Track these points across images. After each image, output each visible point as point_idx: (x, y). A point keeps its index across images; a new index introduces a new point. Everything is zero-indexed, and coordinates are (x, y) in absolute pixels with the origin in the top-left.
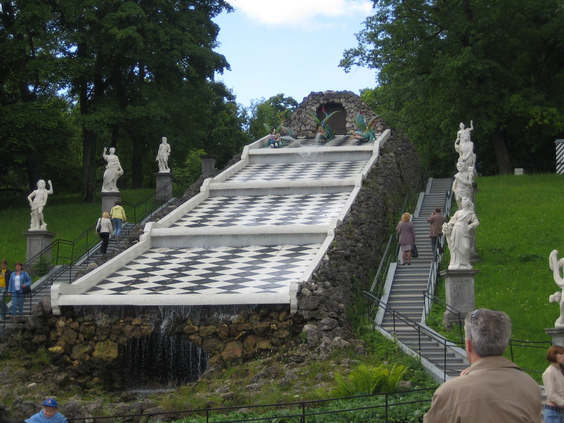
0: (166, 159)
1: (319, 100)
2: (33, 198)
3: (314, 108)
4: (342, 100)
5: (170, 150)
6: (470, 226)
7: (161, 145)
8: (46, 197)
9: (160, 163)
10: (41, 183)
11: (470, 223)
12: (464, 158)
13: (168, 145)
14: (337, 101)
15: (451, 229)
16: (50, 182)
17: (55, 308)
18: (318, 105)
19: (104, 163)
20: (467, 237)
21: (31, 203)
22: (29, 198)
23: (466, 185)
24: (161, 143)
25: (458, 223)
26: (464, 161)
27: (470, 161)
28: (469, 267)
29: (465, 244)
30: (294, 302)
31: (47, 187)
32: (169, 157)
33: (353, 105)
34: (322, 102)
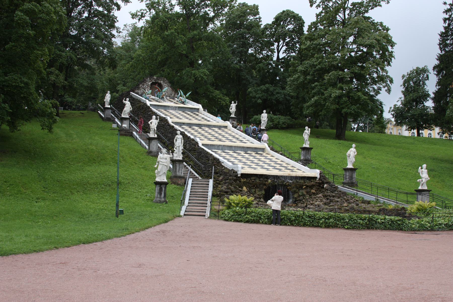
1: (152, 81)
2: (151, 123)
3: (150, 83)
4: (162, 82)
7: (107, 94)
8: (157, 123)
9: (106, 103)
11: (355, 153)
13: (110, 95)
14: (159, 82)
17: (239, 174)
18: (151, 82)
19: (124, 105)
21: (151, 125)
22: (149, 123)
23: (308, 135)
24: (107, 93)
26: (264, 121)
28: (353, 167)
30: (318, 177)
33: (166, 85)
34: (153, 81)
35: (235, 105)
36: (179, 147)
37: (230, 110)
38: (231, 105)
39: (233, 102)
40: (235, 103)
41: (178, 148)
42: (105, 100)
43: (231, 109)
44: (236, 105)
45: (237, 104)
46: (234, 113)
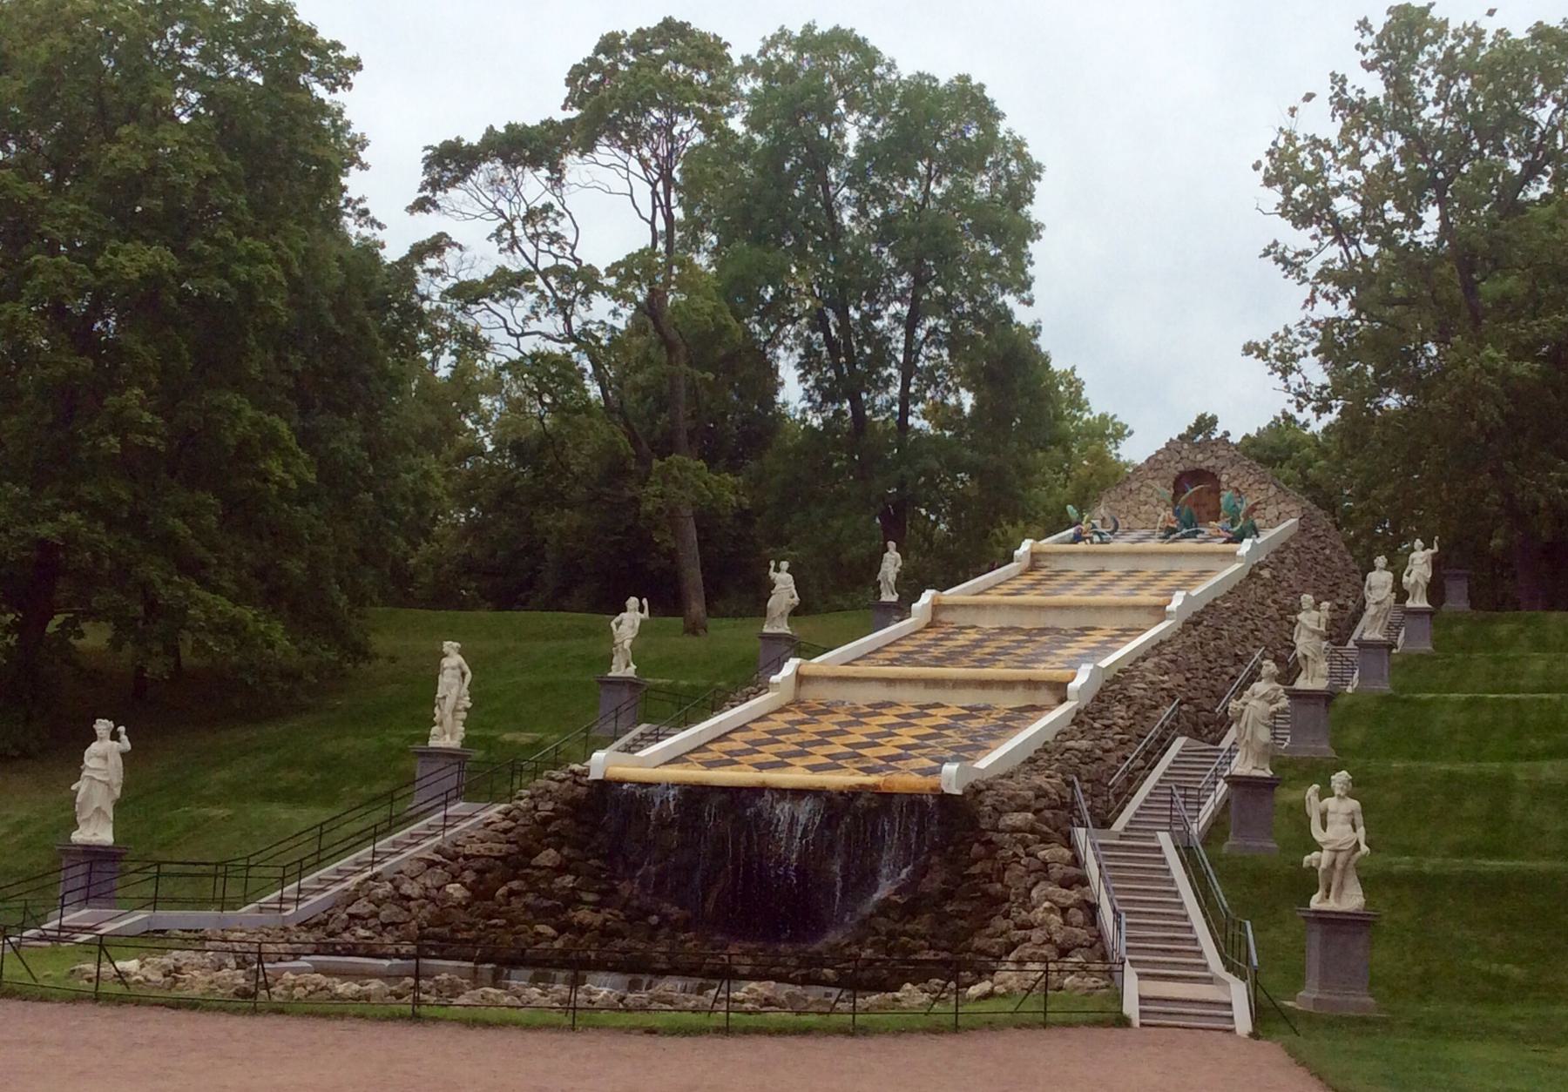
0: (892, 577)
5: (900, 564)
6: (1273, 708)
7: (886, 555)
9: (882, 585)
10: (633, 602)
12: (1379, 599)
13: (898, 555)
15: (1242, 711)
16: (645, 601)
20: (1265, 725)
24: (887, 551)
25: (1253, 703)
27: (1386, 605)
29: (1264, 735)
31: (641, 610)
32: (898, 575)
35: (1429, 551)
36: (444, 698)
37: (1405, 579)
38: (1413, 555)
39: (1418, 543)
40: (1428, 545)
41: (441, 702)
42: (880, 577)
43: (1408, 575)
44: (1434, 555)
45: (1436, 549)
46: (1419, 591)
